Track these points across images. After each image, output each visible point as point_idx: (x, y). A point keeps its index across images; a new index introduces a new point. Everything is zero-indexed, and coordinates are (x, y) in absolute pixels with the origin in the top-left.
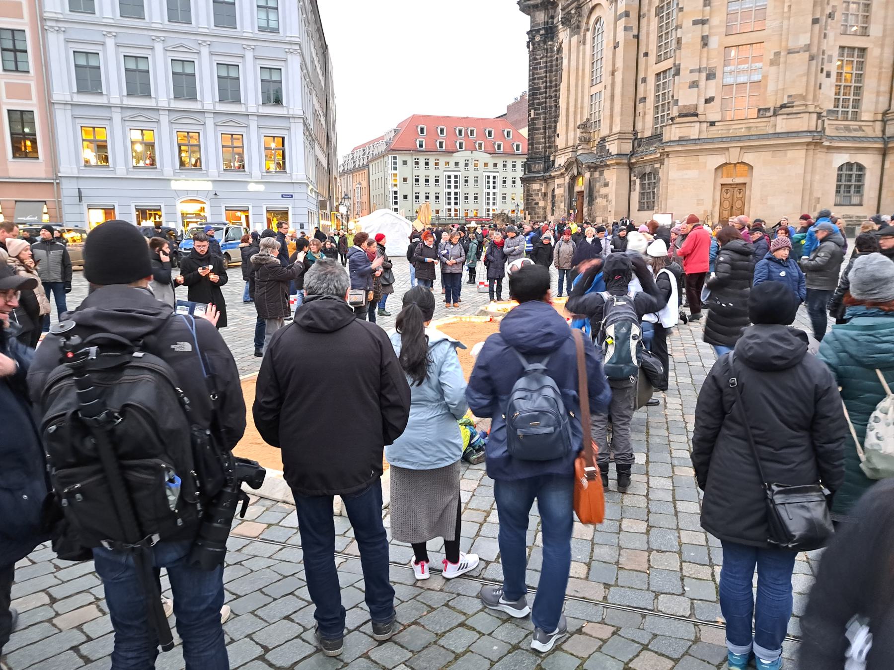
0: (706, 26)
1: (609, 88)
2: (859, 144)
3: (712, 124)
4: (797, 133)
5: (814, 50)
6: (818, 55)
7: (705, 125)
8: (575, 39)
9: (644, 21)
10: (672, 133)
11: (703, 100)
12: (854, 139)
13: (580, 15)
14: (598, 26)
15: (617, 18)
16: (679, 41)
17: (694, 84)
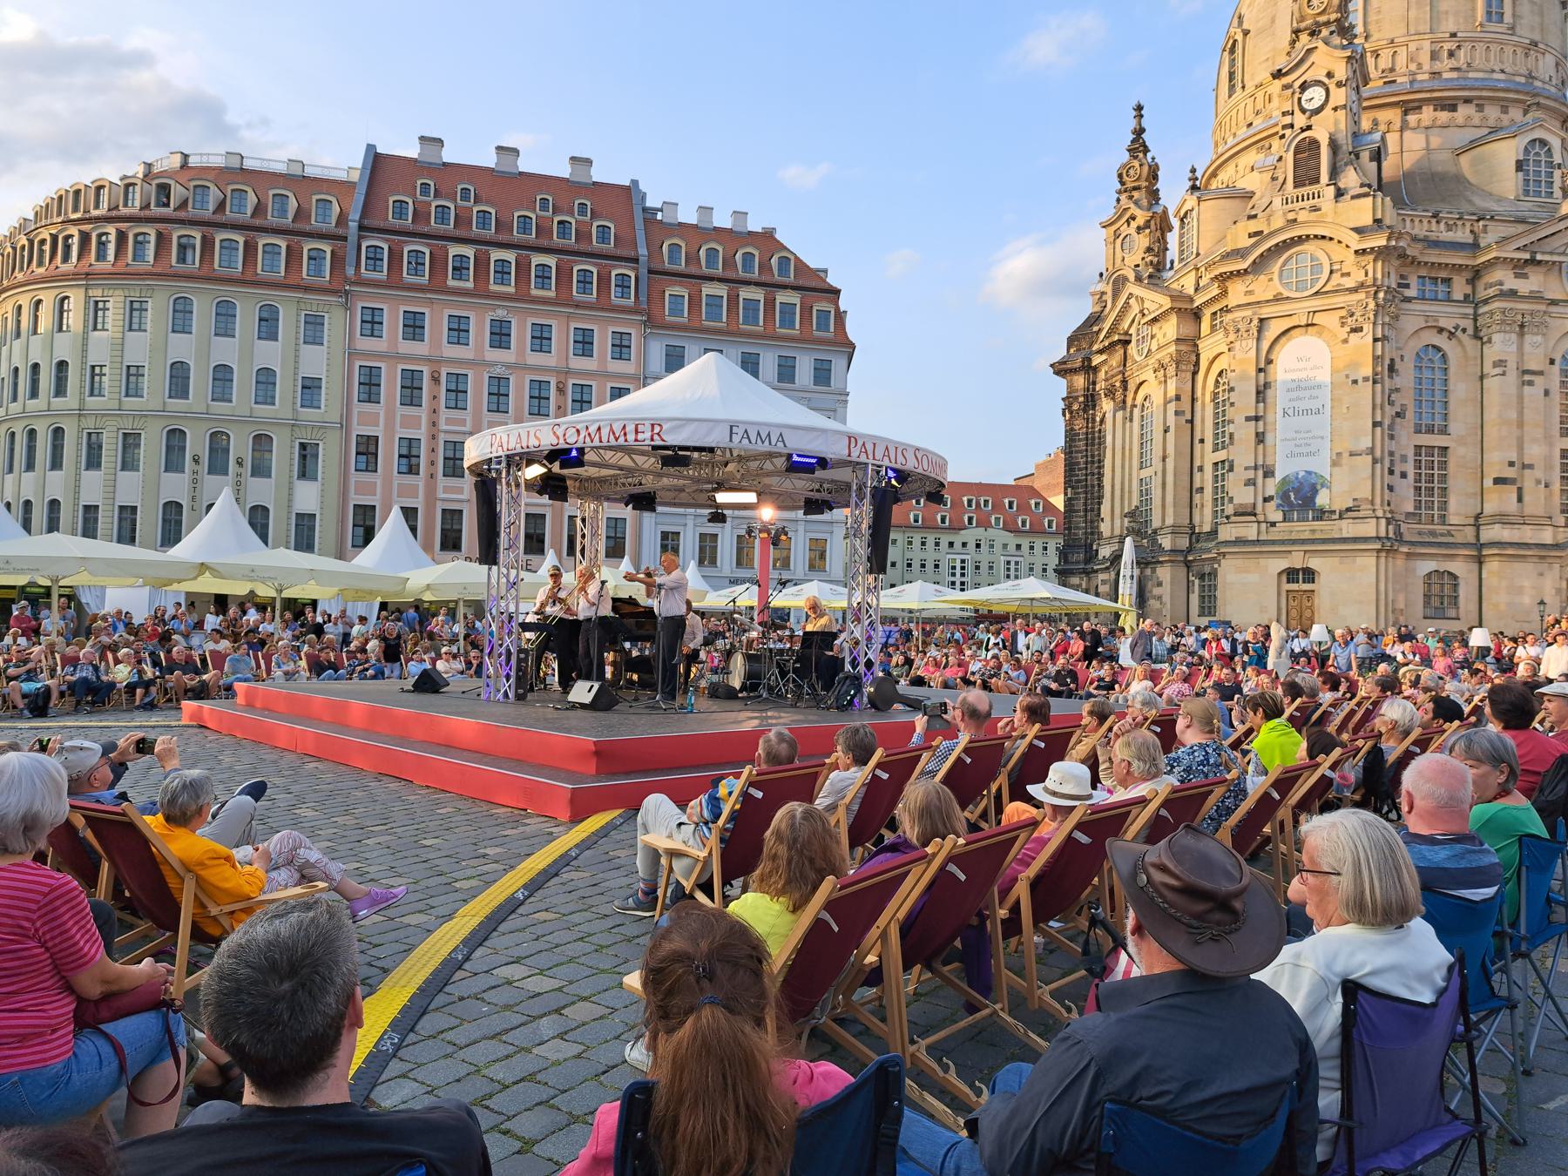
0: (1261, 423)
1: (1160, 474)
2: (1447, 547)
3: (1273, 524)
4: (1365, 540)
5: (1378, 454)
6: (1382, 458)
7: (1263, 526)
8: (1120, 414)
9: (1198, 405)
10: (1226, 533)
11: (1260, 500)
12: (1440, 545)
13: (1125, 389)
14: (1147, 404)
15: (1166, 403)
16: (1231, 435)
17: (1251, 482)
